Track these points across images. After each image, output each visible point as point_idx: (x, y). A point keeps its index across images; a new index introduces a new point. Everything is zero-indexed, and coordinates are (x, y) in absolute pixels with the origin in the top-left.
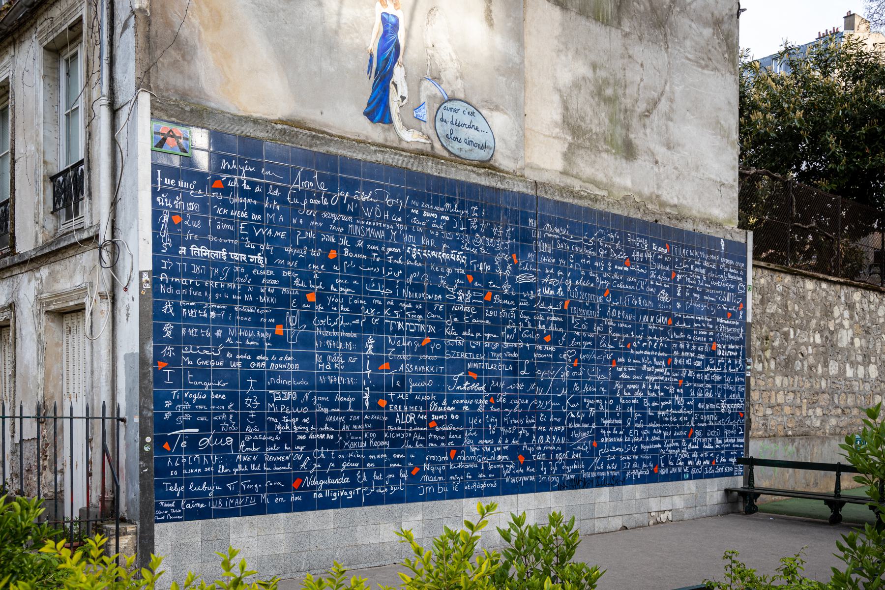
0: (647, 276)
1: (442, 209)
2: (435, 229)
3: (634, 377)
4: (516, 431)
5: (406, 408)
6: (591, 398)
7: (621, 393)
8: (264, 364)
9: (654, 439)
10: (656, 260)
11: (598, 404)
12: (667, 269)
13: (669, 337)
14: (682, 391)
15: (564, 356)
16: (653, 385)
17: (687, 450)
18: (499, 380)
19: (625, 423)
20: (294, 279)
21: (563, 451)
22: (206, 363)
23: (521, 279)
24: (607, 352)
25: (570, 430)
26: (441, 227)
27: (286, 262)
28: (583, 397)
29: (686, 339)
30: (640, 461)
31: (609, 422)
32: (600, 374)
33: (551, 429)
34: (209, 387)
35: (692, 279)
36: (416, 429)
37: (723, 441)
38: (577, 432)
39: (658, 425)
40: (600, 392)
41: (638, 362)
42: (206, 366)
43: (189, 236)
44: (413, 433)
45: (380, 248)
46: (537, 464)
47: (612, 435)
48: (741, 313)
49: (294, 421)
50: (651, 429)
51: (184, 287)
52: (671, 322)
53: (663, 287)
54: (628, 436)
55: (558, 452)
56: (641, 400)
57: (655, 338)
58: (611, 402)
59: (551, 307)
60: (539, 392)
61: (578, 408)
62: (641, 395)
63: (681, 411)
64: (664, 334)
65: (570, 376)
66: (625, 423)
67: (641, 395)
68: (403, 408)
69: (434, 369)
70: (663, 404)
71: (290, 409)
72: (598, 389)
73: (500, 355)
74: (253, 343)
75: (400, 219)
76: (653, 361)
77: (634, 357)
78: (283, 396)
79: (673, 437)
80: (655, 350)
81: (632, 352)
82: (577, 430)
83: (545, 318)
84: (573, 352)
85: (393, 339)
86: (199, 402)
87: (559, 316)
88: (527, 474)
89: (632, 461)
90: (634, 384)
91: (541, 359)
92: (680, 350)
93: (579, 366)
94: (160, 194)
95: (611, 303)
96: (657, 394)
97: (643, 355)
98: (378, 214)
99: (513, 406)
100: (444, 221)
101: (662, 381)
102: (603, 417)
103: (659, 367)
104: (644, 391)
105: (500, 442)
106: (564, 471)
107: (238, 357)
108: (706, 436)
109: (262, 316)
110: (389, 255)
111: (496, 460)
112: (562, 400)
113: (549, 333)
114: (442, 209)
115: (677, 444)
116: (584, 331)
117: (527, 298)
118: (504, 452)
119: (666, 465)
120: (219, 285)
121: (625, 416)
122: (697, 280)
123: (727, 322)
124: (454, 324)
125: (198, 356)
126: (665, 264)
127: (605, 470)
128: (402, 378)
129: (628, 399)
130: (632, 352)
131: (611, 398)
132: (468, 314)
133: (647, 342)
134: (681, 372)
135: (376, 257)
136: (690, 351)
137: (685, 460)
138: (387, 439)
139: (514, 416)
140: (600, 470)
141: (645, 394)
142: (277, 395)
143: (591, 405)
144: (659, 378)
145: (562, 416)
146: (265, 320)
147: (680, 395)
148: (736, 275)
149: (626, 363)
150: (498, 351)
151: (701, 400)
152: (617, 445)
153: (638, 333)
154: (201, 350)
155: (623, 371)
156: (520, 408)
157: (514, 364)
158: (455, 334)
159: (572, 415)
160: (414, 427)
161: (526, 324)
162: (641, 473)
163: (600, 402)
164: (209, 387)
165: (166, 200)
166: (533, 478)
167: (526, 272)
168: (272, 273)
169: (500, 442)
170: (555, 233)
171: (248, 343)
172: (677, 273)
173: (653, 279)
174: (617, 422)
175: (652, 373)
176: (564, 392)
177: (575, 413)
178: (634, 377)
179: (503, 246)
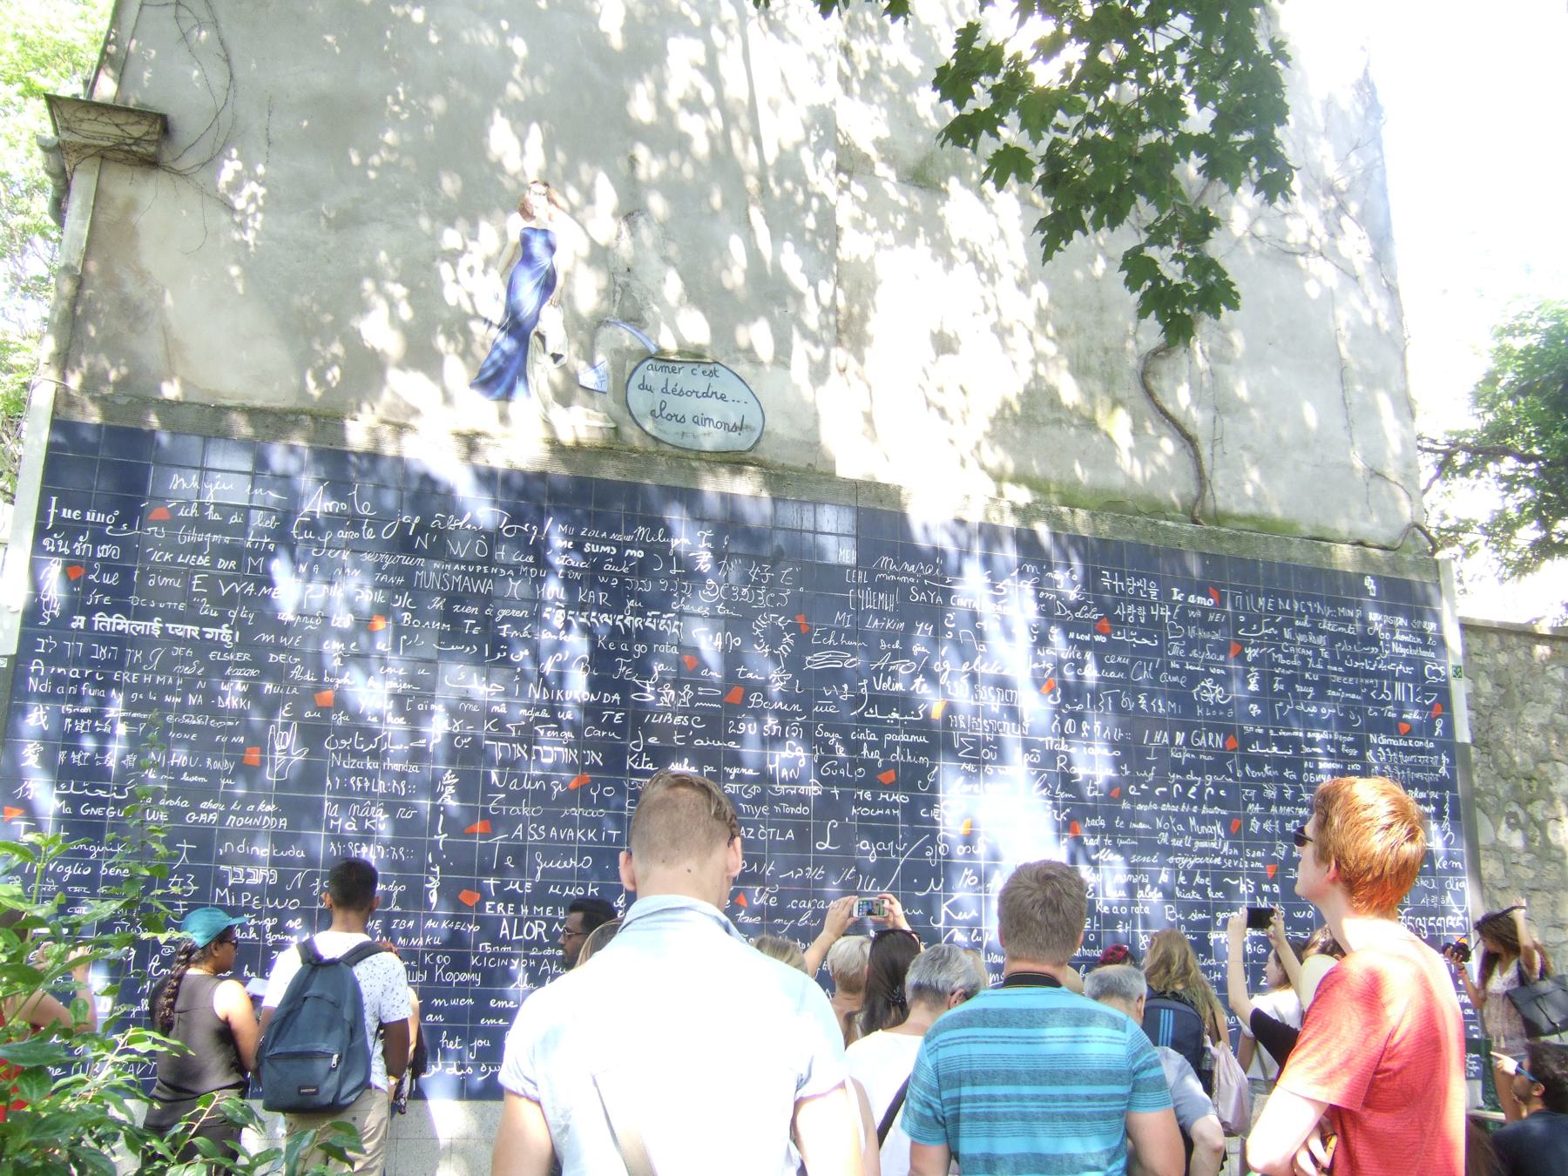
0: (1159, 651)
1: (629, 538)
2: (611, 574)
5: (525, 911)
8: (214, 817)
10: (1184, 619)
12: (1216, 636)
13: (1234, 776)
14: (1277, 889)
16: (1190, 875)
20: (293, 667)
22: (98, 811)
23: (817, 661)
26: (625, 570)
27: (277, 639)
29: (1280, 779)
34: (99, 854)
35: (1289, 656)
36: (548, 952)
42: (97, 817)
43: (95, 598)
44: (539, 960)
45: (482, 611)
48: (1439, 724)
49: (269, 923)
51: (74, 682)
52: (1233, 743)
53: (1208, 674)
57: (1191, 777)
59: (895, 715)
64: (1218, 767)
68: (517, 910)
69: (598, 835)
71: (262, 901)
73: (764, 809)
74: (195, 778)
75: (531, 559)
78: (248, 875)
80: (1191, 803)
81: (1125, 805)
83: (880, 734)
85: (501, 777)
86: (76, 880)
87: (918, 734)
91: (870, 818)
92: (1267, 803)
94: (49, 534)
96: (1205, 896)
97: (1158, 813)
98: (482, 550)
99: (798, 913)
100: (630, 558)
103: (1205, 837)
107: (163, 802)
109: (222, 731)
110: (503, 622)
113: (887, 765)
114: (629, 538)
117: (835, 699)
120: (140, 679)
122: (1303, 658)
123: (1402, 743)
124: (649, 749)
125: (84, 799)
126: (1211, 627)
128: (518, 852)
132: (681, 729)
133: (1170, 787)
134: (1272, 848)
135: (472, 626)
136: (1295, 802)
138: (475, 970)
142: (235, 874)
144: (1209, 860)
146: (224, 740)
148: (1414, 646)
150: (757, 801)
154: (92, 788)
157: (801, 831)
158: (650, 767)
160: (542, 946)
161: (832, 750)
164: (99, 854)
165: (60, 543)
167: (831, 647)
168: (246, 657)
170: (904, 573)
171: (185, 777)
172: (1247, 645)
173: (1176, 657)
179: (772, 600)
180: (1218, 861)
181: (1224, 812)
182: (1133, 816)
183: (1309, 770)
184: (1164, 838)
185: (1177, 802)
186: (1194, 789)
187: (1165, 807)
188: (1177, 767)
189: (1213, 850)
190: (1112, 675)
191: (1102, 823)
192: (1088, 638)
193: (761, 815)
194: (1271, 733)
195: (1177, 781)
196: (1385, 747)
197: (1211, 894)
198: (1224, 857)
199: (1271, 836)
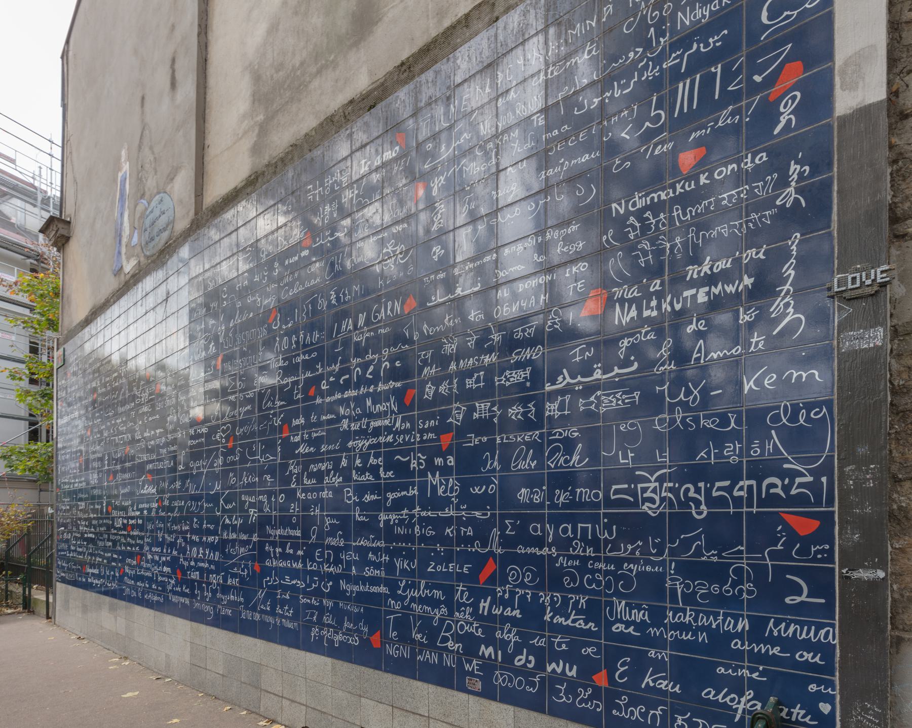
3: (324, 448)
6: (250, 494)
11: (261, 502)
14: (451, 461)
16: (365, 457)
19: (306, 535)
21: (217, 572)
25: (224, 543)
28: (241, 493)
31: (278, 532)
38: (233, 546)
39: (381, 544)
41: (330, 417)
46: (191, 584)
47: (284, 556)
54: (313, 560)
55: (212, 572)
56: (338, 491)
58: (281, 498)
63: (450, 512)
66: (306, 535)
67: (337, 480)
70: (391, 496)
77: (319, 410)
80: (369, 383)
90: (322, 461)
96: (377, 477)
97: (341, 402)
101: (387, 445)
102: (270, 524)
103: (379, 416)
112: (216, 497)
121: (306, 524)
129: (312, 490)
130: (319, 401)
131: (281, 492)
134: (446, 414)
141: (347, 478)
144: (382, 439)
145: (215, 521)
149: (309, 425)
152: (294, 574)
153: (333, 360)
175: (362, 433)
177: (230, 518)
178: (324, 448)
180: (390, 438)
181: (398, 385)
182: (319, 410)
185: (357, 386)
186: (371, 368)
189: (386, 427)
197: (382, 475)
198: (398, 433)
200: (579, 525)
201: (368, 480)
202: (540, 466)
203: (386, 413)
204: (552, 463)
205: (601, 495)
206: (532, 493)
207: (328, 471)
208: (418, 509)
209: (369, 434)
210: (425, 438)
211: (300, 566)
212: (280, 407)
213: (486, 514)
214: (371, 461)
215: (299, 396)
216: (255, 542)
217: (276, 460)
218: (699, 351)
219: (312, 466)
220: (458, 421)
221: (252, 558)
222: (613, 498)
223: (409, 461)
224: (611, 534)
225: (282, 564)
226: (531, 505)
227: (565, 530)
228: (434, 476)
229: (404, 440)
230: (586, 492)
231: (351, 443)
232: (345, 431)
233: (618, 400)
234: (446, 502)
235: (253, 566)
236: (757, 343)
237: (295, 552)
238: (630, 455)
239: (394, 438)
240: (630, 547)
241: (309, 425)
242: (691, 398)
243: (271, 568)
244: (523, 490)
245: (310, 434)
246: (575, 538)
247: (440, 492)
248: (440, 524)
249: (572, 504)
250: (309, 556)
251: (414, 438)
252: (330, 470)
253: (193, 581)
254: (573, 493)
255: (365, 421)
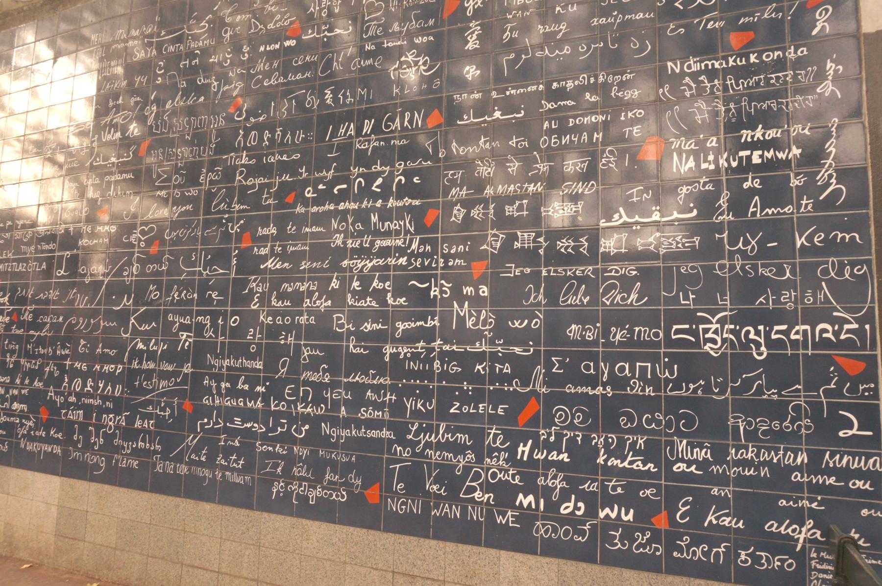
3: (305, 265)
4: (42, 367)
6: (183, 314)
7: (264, 300)
9: (365, 414)
11: (200, 327)
14: (484, 291)
15: (132, 239)
16: (366, 280)
17: (512, 459)
18: (26, 287)
19: (271, 366)
21: (117, 411)
24: (229, 220)
25: (131, 375)
30: (317, 467)
31: (226, 363)
32: (208, 264)
33: (98, 367)
37: (720, 454)
40: (204, 300)
46: (67, 427)
47: (233, 393)
50: (358, 389)
53: (413, 46)
54: (280, 398)
55: (108, 411)
56: (324, 317)
60: (82, 303)
61: (154, 332)
62: (324, 304)
63: (481, 347)
65: (142, 273)
66: (271, 366)
67: (324, 304)
70: (401, 326)
72: (201, 294)
73: (33, 248)
76: (366, 221)
77: (301, 221)
79: (443, 413)
80: (375, 196)
81: (300, 209)
82: (149, 374)
84: (152, 229)
87: (127, 172)
88: (49, 440)
89: (291, 460)
90: (302, 280)
93: (163, 253)
95: (247, 119)
96: (384, 303)
101: (397, 267)
103: (388, 234)
104: (337, 297)
105: (18, 381)
106: (118, 449)
108: (611, 425)
111: (10, 409)
115: (463, 438)
116: (175, 187)
118: (21, 399)
119: (415, 487)
121: (272, 354)
127: (211, 463)
130: (300, 209)
131: (234, 313)
137: (504, 495)
139: (41, 342)
140: (200, 464)
143: (184, 328)
144: (391, 261)
145: (121, 346)
147: (477, 301)
151: (582, 317)
155: (272, 253)
156: (50, 330)
159: (141, 346)
162: (318, 492)
163: (207, 321)
166: (58, 450)
169: (18, 381)
174: (248, 364)
175: (363, 253)
176: (127, 302)
177: (146, 343)
178: (305, 265)
180: (403, 261)
181: (417, 203)
182: (301, 221)
183: (550, 132)
184: (338, 239)
185: (358, 199)
186: (380, 181)
187: (342, 206)
188: (364, 160)
190: (299, 76)
191: (274, 231)
192: (277, 46)
193: (31, 253)
194: (494, 95)
195: (359, 176)
196: (695, 76)
197: (390, 301)
199: (482, 225)
200: (638, 364)
201: (368, 306)
202: (594, 302)
203: (398, 233)
204: (607, 299)
205: (661, 335)
206: (584, 329)
207: (310, 294)
208: (439, 342)
209: (373, 254)
210: (450, 264)
211: (260, 404)
212: (239, 211)
213: (529, 351)
214: (374, 284)
215: (270, 201)
216: (186, 375)
217: (229, 274)
218: (755, 206)
219: (285, 285)
220: (495, 249)
221: (181, 394)
222: (674, 337)
223: (429, 288)
224: (672, 374)
225: (229, 403)
226: (584, 342)
227: (622, 369)
228: (461, 306)
229: (422, 264)
230: (645, 331)
231: (346, 262)
232: (337, 247)
233: (678, 243)
234: (478, 335)
235: (180, 405)
236: (807, 205)
237: (252, 388)
238: (691, 297)
239: (409, 260)
240: (692, 386)
241: (282, 236)
242: (750, 247)
243: (212, 408)
244: (573, 326)
245: (284, 247)
246: (633, 377)
247: (469, 324)
248: (467, 360)
249: (629, 342)
250: (275, 391)
251: (437, 262)
252: (314, 292)
253: (71, 423)
254: (631, 331)
255: (368, 239)
